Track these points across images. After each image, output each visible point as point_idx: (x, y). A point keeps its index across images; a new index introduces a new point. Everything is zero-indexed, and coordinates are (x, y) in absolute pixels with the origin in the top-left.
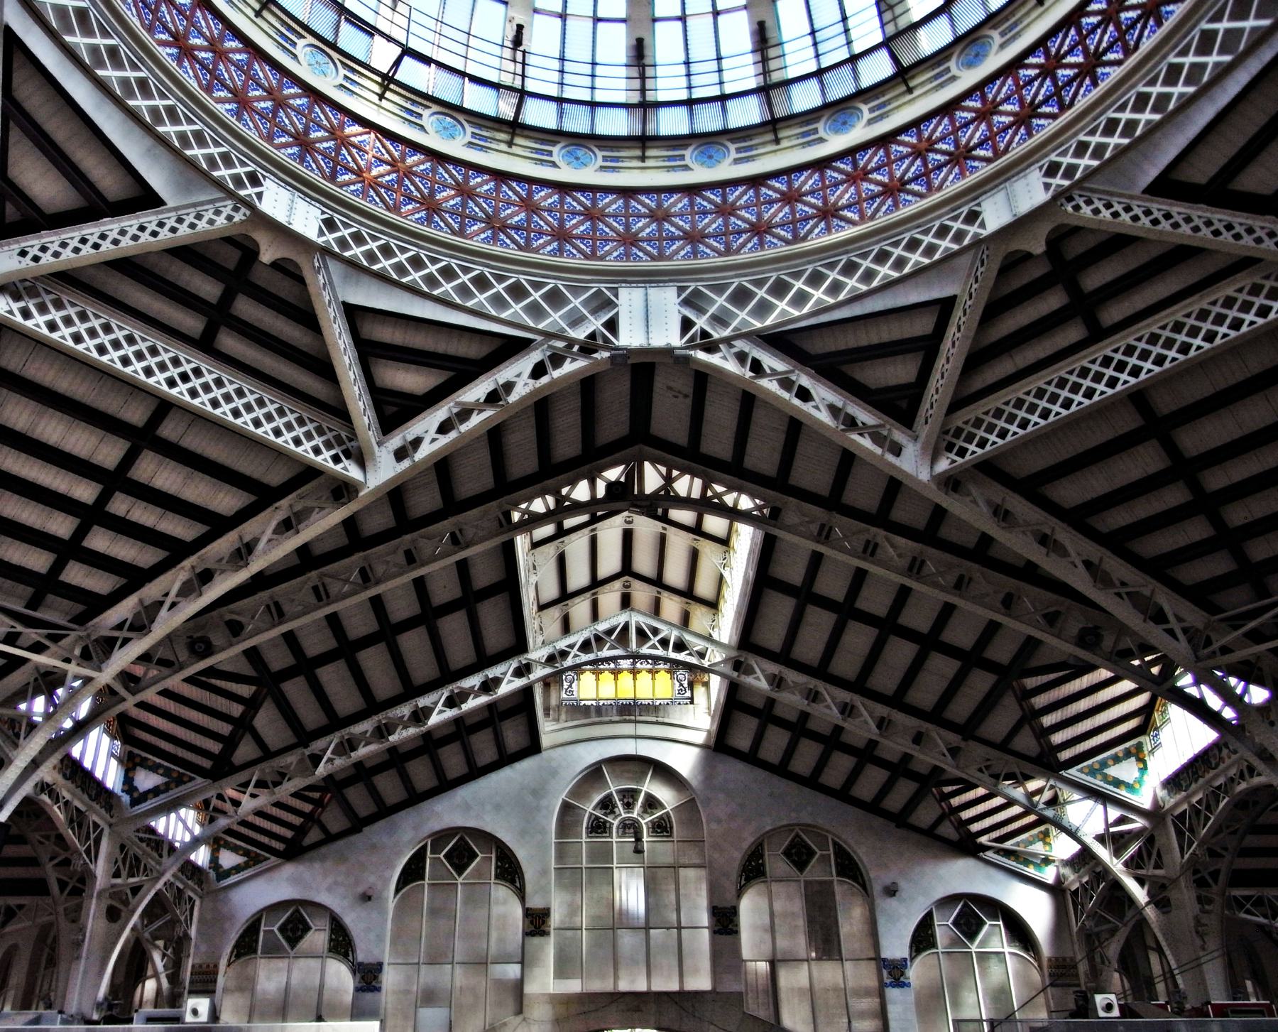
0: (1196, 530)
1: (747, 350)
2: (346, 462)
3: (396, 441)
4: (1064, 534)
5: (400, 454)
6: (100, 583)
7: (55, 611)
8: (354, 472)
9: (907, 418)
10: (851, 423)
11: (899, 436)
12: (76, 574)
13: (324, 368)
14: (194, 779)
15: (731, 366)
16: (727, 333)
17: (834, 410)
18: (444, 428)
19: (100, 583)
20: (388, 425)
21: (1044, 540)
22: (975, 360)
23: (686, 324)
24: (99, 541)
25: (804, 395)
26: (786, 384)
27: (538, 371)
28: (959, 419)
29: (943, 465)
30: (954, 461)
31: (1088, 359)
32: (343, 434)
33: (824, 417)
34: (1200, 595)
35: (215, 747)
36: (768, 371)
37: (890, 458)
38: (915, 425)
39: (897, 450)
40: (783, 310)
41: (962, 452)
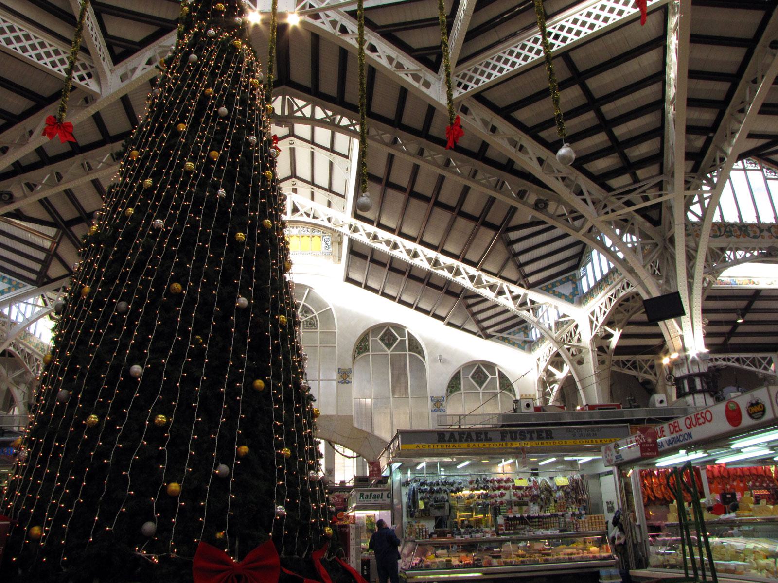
1: (337, 19)
2: (88, 80)
3: (121, 69)
4: (526, 140)
5: (123, 78)
9: (434, 67)
11: (429, 75)
14: (26, 286)
15: (328, 27)
16: (324, 5)
17: (390, 59)
21: (514, 144)
30: (460, 93)
32: (87, 64)
33: (384, 62)
34: (601, 180)
35: (37, 267)
36: (350, 32)
37: (423, 89)
38: (439, 71)
39: (427, 85)
41: (466, 87)
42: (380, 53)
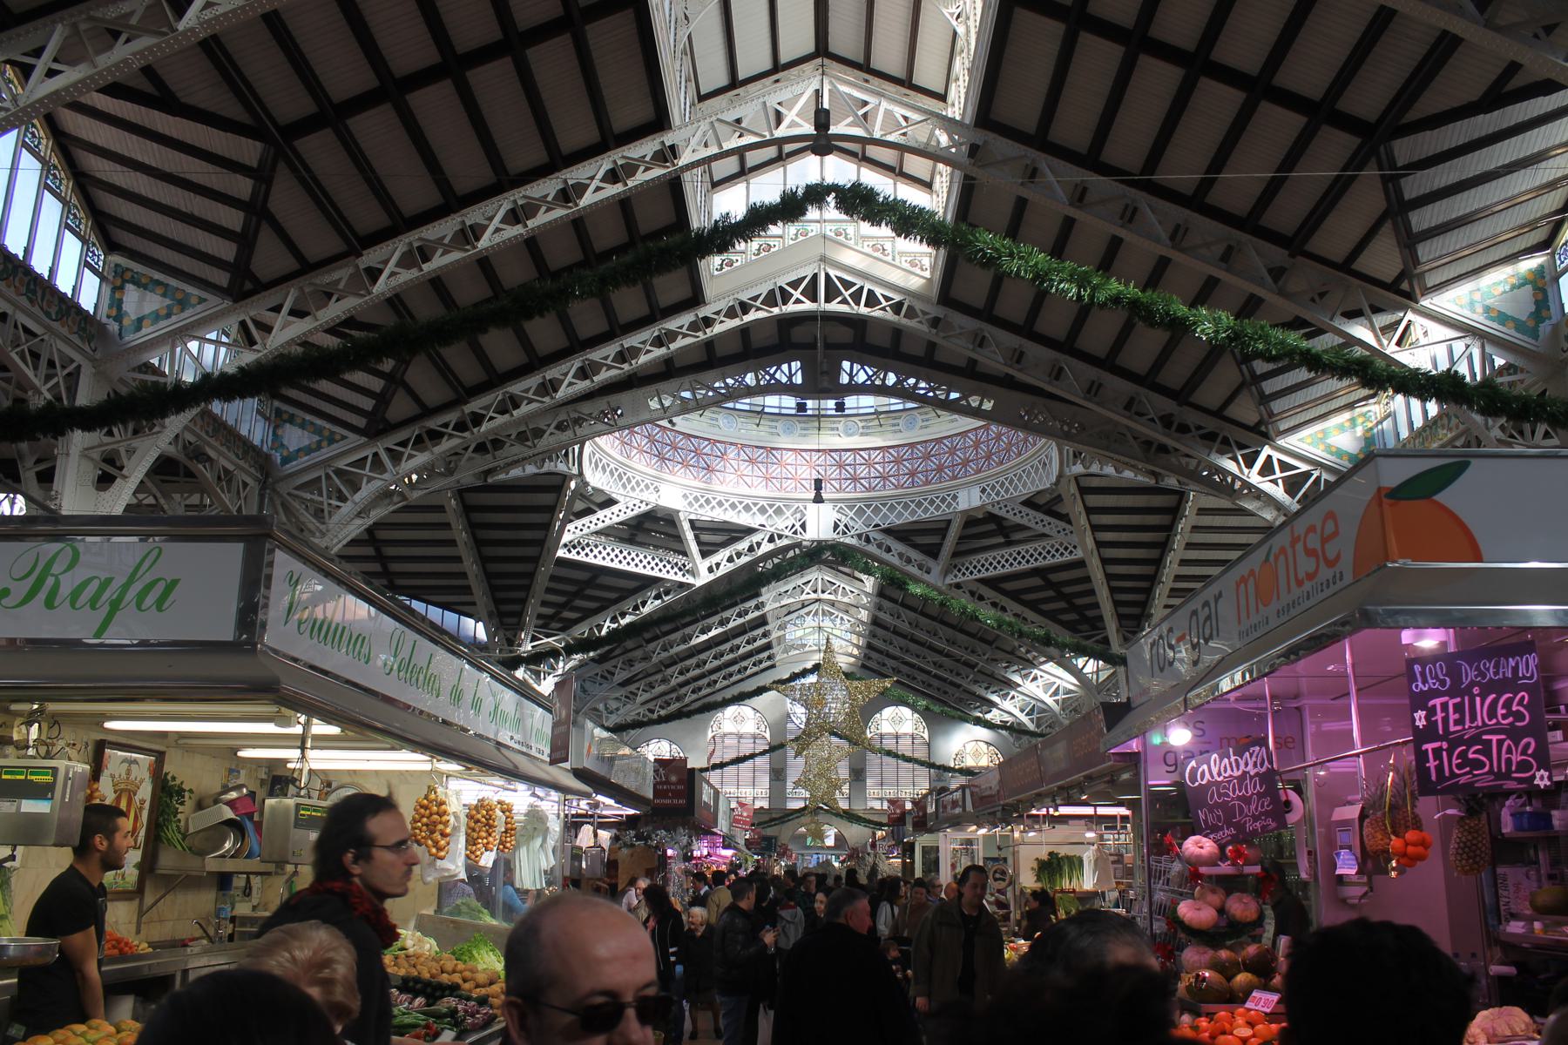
0: (1062, 605)
5: (710, 570)
6: (573, 615)
7: (555, 625)
8: (689, 579)
10: (909, 561)
11: (930, 562)
12: (567, 614)
13: (679, 538)
17: (901, 555)
18: (730, 560)
19: (573, 615)
20: (704, 555)
22: (962, 538)
23: (836, 526)
24: (578, 603)
25: (889, 550)
26: (879, 546)
27: (771, 540)
28: (957, 561)
29: (950, 580)
31: (1005, 552)
40: (877, 521)
42: (894, 552)
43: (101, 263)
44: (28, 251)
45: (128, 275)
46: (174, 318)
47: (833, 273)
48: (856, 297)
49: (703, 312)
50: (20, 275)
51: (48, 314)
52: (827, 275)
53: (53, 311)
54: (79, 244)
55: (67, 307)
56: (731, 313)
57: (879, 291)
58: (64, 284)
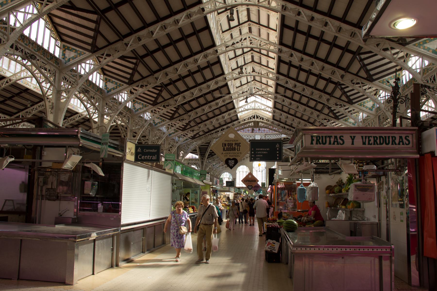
43: (60, 45)
44: (43, 44)
45: (66, 48)
46: (117, 89)
47: (257, 115)
48: (261, 118)
49: (239, 121)
50: (41, 50)
51: (48, 59)
52: (257, 115)
53: (49, 58)
54: (54, 40)
55: (52, 56)
56: (243, 121)
57: (264, 117)
58: (51, 51)
